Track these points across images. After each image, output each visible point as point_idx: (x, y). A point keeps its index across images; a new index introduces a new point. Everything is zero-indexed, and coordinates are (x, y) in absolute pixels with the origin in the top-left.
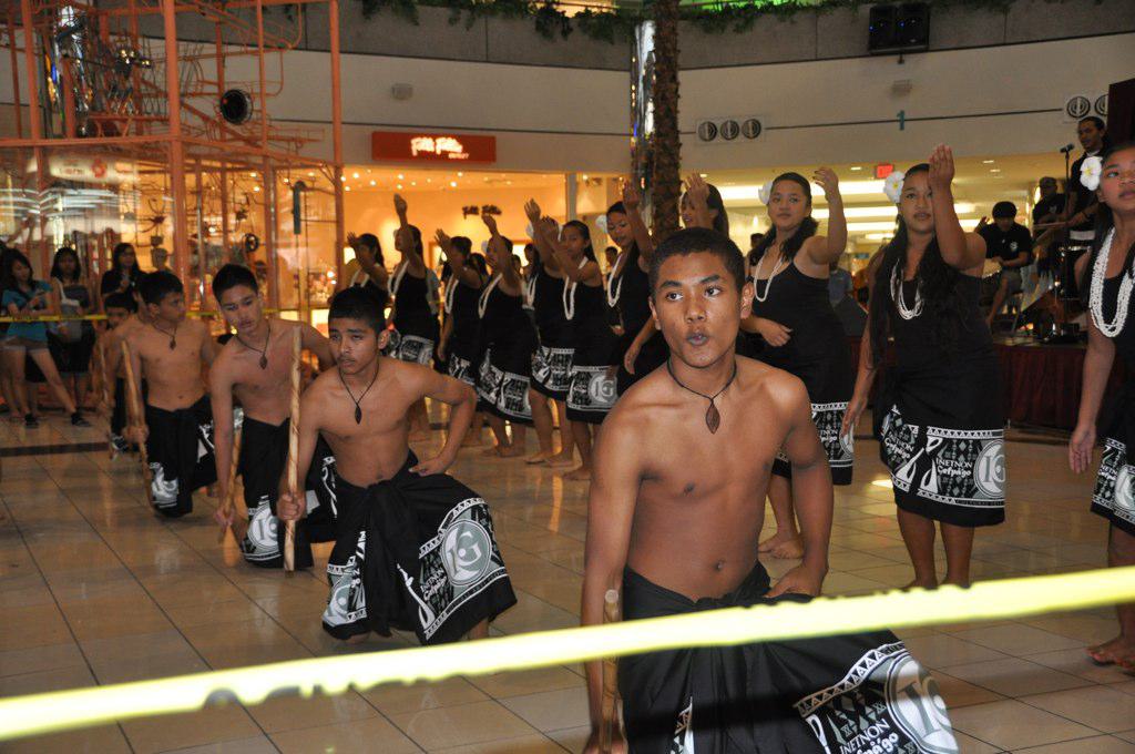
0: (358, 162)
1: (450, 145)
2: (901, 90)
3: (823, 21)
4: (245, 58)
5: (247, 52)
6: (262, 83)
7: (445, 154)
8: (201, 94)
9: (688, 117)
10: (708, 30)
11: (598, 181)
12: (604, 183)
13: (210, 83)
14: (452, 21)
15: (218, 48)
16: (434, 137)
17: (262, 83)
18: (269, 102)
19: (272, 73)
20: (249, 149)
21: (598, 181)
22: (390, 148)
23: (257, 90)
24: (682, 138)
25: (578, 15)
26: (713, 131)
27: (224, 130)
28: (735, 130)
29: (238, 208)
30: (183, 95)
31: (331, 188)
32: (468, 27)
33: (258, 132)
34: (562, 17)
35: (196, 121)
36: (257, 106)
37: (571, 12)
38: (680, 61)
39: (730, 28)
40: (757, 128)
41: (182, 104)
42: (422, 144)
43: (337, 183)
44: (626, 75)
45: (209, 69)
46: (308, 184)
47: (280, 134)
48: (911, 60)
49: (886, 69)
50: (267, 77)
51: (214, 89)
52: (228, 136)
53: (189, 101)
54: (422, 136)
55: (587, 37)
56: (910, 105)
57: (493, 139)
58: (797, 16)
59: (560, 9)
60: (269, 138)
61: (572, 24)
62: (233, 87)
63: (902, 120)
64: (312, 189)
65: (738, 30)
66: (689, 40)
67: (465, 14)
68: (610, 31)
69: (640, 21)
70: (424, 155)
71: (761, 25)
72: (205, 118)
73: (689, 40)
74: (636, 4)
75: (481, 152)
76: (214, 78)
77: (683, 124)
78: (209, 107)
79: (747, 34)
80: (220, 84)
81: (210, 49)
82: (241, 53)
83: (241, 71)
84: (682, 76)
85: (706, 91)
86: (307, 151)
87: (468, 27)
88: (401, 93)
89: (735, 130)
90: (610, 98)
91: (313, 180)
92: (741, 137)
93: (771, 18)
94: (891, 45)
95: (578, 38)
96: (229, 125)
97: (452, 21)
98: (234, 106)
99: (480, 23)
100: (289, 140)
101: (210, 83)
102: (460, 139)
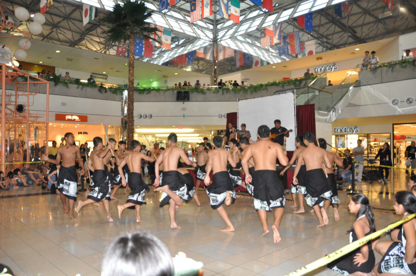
0: (52, 122)
1: (76, 118)
2: (184, 109)
3: (167, 93)
4: (24, 96)
5: (24, 95)
6: (28, 102)
7: (74, 120)
8: (10, 104)
9: (135, 113)
10: (140, 93)
11: (113, 127)
12: (114, 128)
13: (13, 102)
14: (77, 88)
15: (16, 93)
16: (72, 115)
17: (28, 102)
18: (30, 107)
19: (31, 100)
20: (23, 119)
21: (113, 127)
22: (60, 117)
23: (26, 104)
24: (135, 119)
25: (109, 88)
26: (141, 116)
27: (16, 114)
28: (146, 116)
29: (19, 133)
30: (6, 105)
31: (45, 129)
32: (82, 89)
33: (26, 114)
34: (105, 88)
35: (9, 112)
36: (26, 108)
37: (107, 88)
38: (134, 101)
39: (145, 93)
40: (151, 116)
41: (6, 107)
42: (69, 117)
43: (47, 127)
44: (120, 103)
45: (13, 98)
46: (39, 128)
47: (32, 115)
48: (186, 103)
49: (180, 104)
50: (30, 101)
51: (14, 103)
52: (17, 115)
53: (8, 106)
54: (69, 115)
55: (111, 93)
56: (186, 113)
57: (87, 116)
58: (161, 92)
59: (105, 86)
60: (29, 117)
61: (108, 90)
62: (19, 104)
63: (184, 116)
64: (40, 129)
65: (147, 94)
66: (136, 95)
67: (81, 86)
68: (117, 91)
69: (124, 90)
70: (69, 120)
71: (152, 93)
72: (11, 111)
73: (136, 95)
74: (122, 85)
75: (83, 119)
76: (14, 100)
77: (135, 115)
78: (13, 108)
79: (149, 95)
80: (16, 102)
81: (13, 92)
82: (22, 95)
83: (22, 100)
84: (135, 104)
85: (140, 107)
86: (39, 120)
87: (82, 89)
88: (64, 104)
89: (146, 116)
90: (115, 108)
91: (40, 127)
92: (147, 118)
93: (155, 91)
94: (181, 99)
95: (108, 93)
96: (18, 113)
97: (77, 88)
98: (20, 108)
99: (85, 88)
100: (34, 117)
101: (13, 102)
102: (78, 116)
